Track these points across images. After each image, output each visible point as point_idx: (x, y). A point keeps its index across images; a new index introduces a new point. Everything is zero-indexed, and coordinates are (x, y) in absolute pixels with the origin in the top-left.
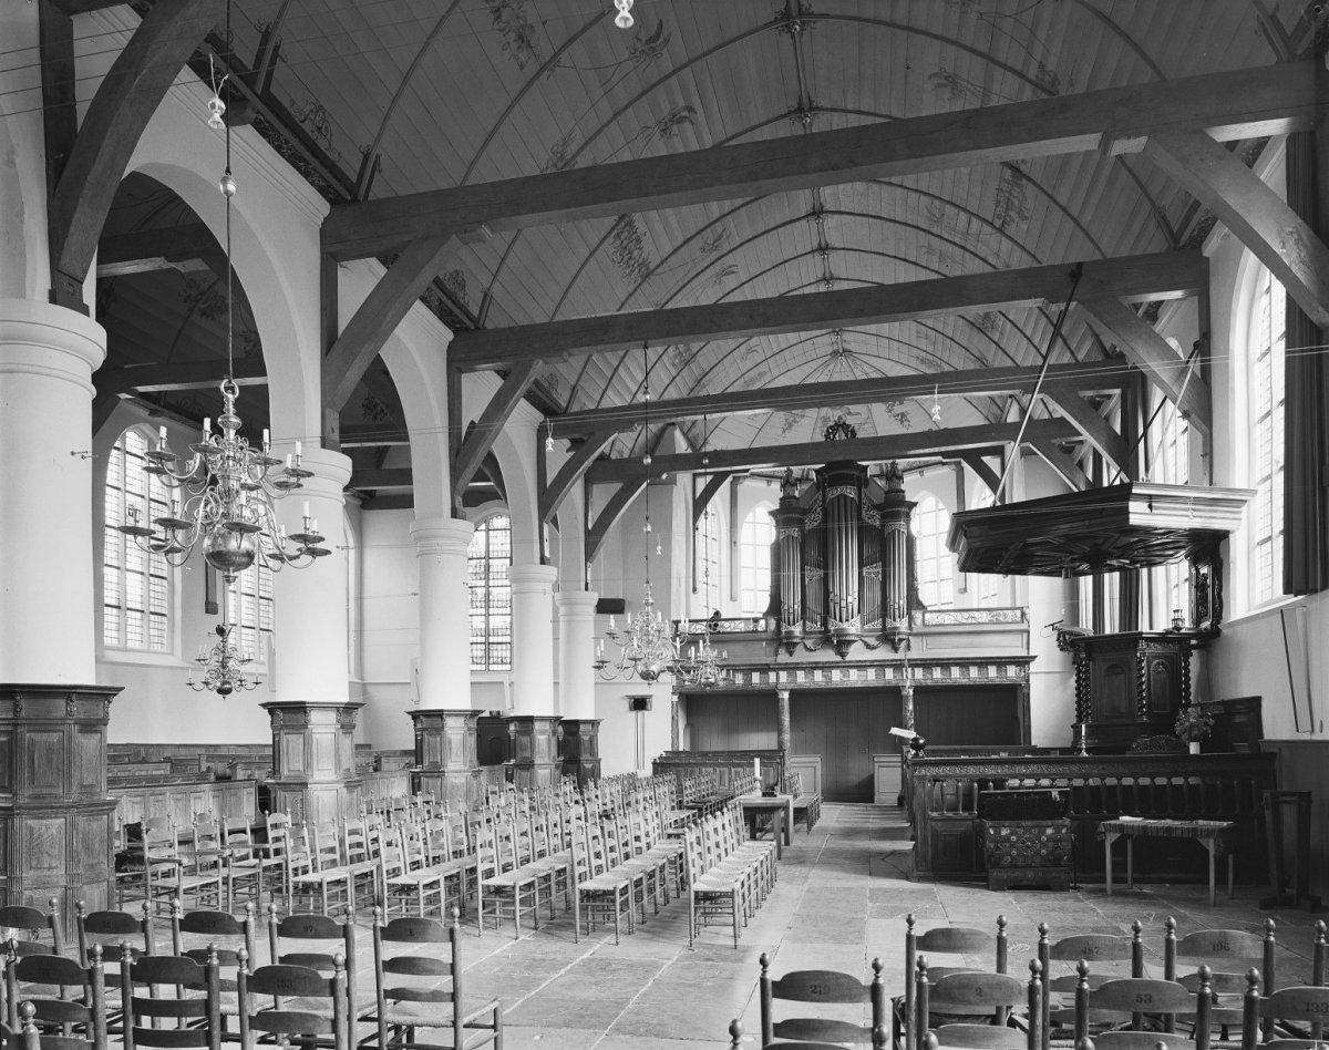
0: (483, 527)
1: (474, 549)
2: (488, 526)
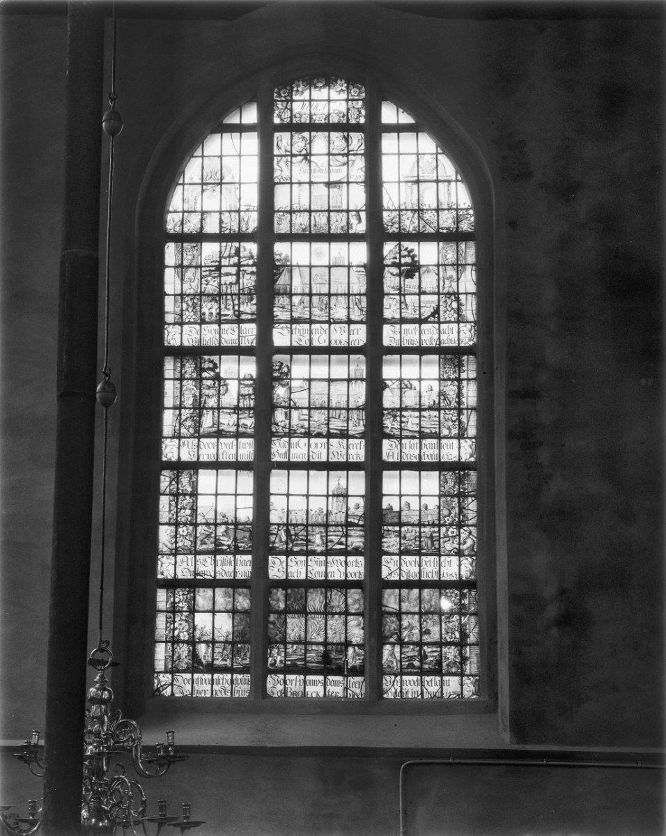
0: (250, 115)
1: (211, 201)
2: (266, 113)
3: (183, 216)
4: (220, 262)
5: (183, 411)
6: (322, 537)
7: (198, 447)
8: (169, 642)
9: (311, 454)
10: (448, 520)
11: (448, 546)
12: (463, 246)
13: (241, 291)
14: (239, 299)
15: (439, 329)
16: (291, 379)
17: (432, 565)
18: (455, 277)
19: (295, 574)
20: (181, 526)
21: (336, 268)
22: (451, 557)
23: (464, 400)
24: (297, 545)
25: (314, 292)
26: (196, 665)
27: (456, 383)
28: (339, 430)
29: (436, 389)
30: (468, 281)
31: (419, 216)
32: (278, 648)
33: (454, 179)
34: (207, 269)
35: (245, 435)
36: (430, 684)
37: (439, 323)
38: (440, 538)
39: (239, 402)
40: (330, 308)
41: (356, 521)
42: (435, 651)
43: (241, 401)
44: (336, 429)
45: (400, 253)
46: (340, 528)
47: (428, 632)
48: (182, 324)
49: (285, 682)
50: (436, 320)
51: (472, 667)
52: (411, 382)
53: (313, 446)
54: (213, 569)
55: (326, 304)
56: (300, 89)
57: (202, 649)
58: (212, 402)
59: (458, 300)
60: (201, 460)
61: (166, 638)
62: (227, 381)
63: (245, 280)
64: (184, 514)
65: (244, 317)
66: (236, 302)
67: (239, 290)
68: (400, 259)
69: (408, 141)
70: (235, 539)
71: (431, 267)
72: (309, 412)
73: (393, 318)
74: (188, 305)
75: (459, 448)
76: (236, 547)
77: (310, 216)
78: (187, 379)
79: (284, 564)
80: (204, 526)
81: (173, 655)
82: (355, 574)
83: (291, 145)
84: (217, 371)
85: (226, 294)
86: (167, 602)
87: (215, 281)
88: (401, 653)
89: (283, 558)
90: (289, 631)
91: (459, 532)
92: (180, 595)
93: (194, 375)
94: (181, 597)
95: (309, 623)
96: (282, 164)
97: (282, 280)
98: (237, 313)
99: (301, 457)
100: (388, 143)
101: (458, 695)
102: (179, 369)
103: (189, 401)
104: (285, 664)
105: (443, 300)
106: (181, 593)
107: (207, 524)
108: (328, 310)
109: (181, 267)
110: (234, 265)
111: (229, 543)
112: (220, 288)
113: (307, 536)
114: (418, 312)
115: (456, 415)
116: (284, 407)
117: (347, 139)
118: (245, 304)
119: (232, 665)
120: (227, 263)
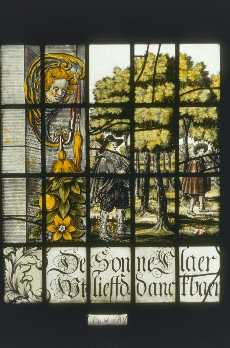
4: (132, 95)
13: (182, 167)
14: (178, 187)
48: (45, 245)
63: (190, 141)
65: (188, 230)
66: (171, 194)
67: (177, 163)
74: (58, 199)
85: (148, 175)
87: (119, 142)
110: (164, 103)
112: (131, 159)
118: (192, 200)
120: (148, 99)
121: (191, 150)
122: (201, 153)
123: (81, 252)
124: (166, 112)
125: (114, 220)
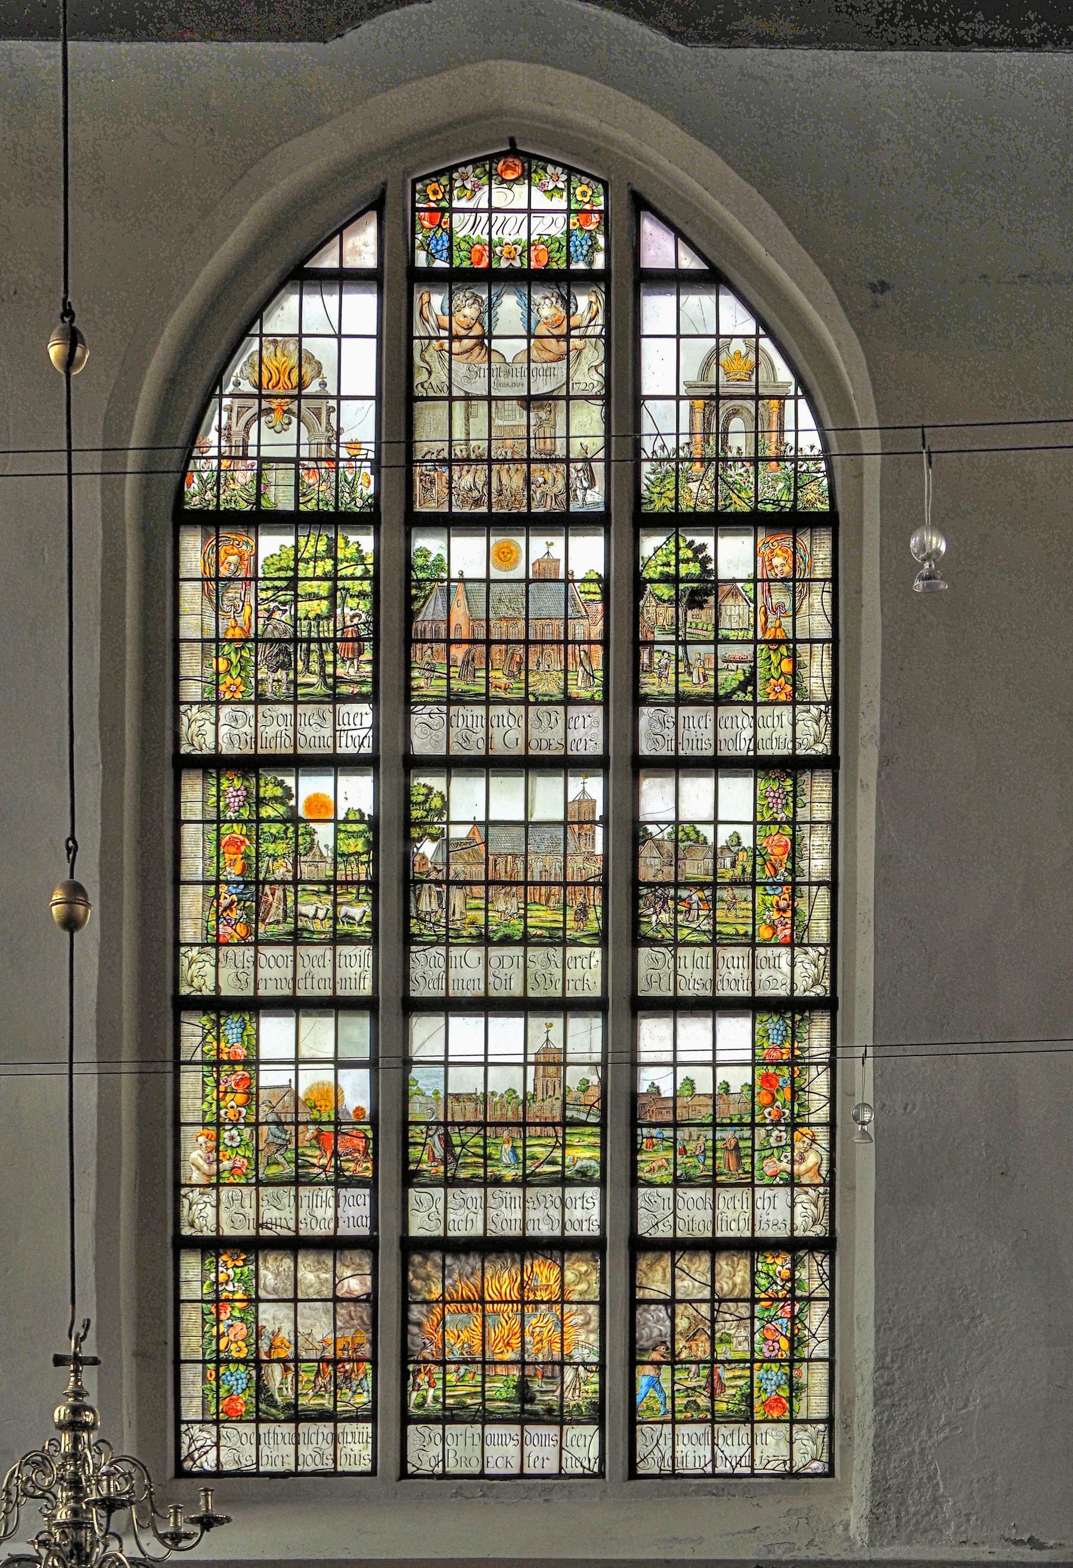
0: (362, 247)
2: (396, 243)
3: (220, 464)
4: (295, 569)
5: (223, 888)
6: (514, 1148)
7: (256, 963)
8: (210, 1361)
9: (491, 979)
10: (768, 1114)
11: (770, 1167)
12: (804, 540)
13: (339, 634)
14: (335, 651)
15: (754, 717)
16: (448, 823)
17: (738, 1205)
18: (788, 604)
19: (462, 1226)
20: (228, 1127)
21: (541, 585)
22: (776, 1189)
23: (804, 864)
24: (465, 1166)
25: (494, 637)
26: (263, 1409)
27: (788, 830)
28: (547, 929)
29: (747, 842)
30: (815, 618)
31: (717, 475)
32: (429, 1373)
33: (792, 393)
34: (269, 584)
35: (349, 939)
36: (729, 1442)
37: (755, 704)
38: (754, 1150)
39: (335, 870)
40: (527, 671)
41: (583, 1117)
42: (740, 1377)
43: (341, 866)
44: (541, 928)
45: (677, 554)
46: (550, 1130)
47: (727, 1340)
48: (218, 703)
49: (444, 1439)
50: (749, 698)
51: (814, 1404)
52: (699, 827)
53: (494, 962)
54: (293, 1216)
55: (519, 664)
56: (469, 186)
57: (275, 1374)
58: (281, 870)
59: (794, 656)
60: (262, 992)
61: (204, 1354)
62: (312, 825)
63: (347, 610)
64: (232, 1103)
65: (344, 689)
66: (329, 657)
67: (335, 631)
68: (677, 566)
69: (698, 305)
70: (336, 1154)
71: (739, 585)
72: (487, 892)
73: (662, 693)
75: (793, 966)
76: (338, 1170)
77: (490, 470)
78: (231, 821)
79: (441, 1205)
80: (273, 1127)
81: (218, 1387)
82: (581, 1223)
83: (451, 315)
84: (292, 803)
85: (309, 640)
86: (203, 1282)
88: (674, 1383)
89: (439, 1192)
90: (450, 1339)
91: (792, 1139)
92: (230, 1269)
93: (245, 814)
94: (230, 1272)
95: (489, 1321)
96: (431, 356)
97: (430, 613)
98: (330, 681)
99: (470, 986)
100: (658, 310)
101: (785, 1462)
102: (214, 799)
103: (232, 872)
104: (444, 1403)
105: (764, 655)
106: (230, 1264)
107: (279, 1123)
108: (523, 677)
109: (215, 583)
111: (324, 1161)
112: (295, 627)
113: (485, 1148)
114: (711, 681)
115: (787, 896)
116: (438, 883)
117: (567, 303)
119: (335, 1406)
120: (310, 573)
121: (348, 618)
122: (356, 621)
123: (250, 710)
124: (327, 584)
125: (278, 681)
